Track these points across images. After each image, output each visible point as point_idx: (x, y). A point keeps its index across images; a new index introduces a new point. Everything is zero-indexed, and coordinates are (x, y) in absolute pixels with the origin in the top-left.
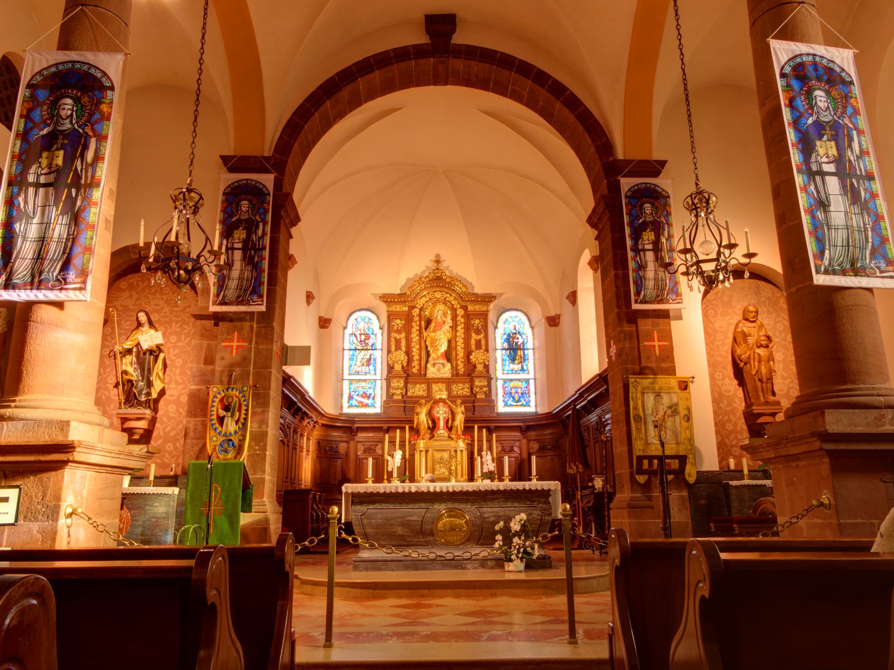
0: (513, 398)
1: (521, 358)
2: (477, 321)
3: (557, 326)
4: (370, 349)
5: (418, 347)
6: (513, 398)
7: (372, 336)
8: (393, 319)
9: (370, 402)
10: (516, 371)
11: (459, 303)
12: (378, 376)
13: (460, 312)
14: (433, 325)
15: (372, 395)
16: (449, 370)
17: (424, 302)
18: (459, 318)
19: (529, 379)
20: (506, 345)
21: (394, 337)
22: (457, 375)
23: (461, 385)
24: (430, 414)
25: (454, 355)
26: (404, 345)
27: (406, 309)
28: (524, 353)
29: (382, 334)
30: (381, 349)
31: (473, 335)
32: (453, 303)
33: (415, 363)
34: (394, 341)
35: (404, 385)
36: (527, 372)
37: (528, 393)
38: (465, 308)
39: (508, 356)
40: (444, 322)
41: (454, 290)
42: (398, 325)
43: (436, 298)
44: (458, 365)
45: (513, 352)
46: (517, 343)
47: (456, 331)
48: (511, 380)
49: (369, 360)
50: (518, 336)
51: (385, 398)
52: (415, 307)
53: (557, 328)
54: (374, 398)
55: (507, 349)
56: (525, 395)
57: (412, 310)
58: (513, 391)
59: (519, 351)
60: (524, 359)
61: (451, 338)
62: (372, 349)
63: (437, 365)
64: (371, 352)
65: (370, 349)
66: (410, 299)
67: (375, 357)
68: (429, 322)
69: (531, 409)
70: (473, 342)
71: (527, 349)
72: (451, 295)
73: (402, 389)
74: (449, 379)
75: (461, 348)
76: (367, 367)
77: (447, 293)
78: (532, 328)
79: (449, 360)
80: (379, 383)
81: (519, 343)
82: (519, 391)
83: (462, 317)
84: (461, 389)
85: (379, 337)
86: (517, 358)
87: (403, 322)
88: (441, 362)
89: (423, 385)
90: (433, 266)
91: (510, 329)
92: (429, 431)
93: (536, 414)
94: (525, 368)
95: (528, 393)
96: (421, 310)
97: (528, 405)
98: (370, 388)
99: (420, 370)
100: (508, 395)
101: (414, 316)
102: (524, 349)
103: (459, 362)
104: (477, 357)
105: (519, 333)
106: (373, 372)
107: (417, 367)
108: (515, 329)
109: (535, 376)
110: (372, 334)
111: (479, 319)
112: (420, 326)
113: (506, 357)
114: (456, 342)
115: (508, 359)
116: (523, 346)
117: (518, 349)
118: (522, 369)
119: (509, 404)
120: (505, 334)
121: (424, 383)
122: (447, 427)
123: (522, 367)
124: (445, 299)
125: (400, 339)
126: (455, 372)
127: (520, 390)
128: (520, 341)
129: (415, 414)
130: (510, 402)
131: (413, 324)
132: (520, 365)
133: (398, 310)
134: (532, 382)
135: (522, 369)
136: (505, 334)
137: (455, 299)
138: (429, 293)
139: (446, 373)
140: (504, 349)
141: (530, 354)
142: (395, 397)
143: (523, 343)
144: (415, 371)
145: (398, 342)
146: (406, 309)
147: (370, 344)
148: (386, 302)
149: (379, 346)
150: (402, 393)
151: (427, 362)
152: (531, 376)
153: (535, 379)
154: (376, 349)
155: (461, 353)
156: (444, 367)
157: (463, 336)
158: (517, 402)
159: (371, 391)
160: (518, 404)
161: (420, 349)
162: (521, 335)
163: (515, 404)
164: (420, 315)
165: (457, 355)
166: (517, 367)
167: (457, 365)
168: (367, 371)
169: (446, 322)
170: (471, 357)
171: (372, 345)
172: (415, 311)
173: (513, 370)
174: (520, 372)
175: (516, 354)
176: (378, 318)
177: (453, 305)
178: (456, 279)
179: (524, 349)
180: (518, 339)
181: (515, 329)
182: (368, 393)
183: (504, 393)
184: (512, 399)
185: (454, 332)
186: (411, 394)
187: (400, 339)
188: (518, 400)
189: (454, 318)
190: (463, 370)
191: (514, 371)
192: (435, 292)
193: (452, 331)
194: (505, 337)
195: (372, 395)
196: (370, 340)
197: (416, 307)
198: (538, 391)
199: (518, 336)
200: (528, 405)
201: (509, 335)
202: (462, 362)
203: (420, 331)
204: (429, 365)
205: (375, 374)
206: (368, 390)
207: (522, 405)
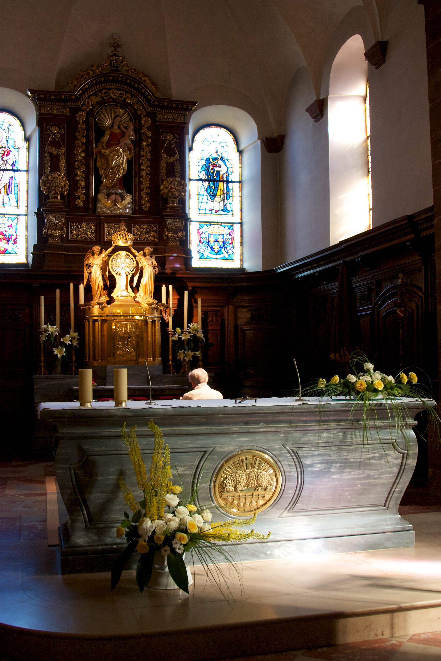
0: (212, 248)
1: (224, 193)
2: (170, 137)
3: (277, 152)
4: (9, 170)
5: (83, 168)
6: (212, 248)
7: (12, 150)
8: (47, 125)
9: (10, 246)
10: (217, 211)
11: (144, 108)
12: (23, 210)
13: (146, 122)
14: (106, 138)
15: (14, 238)
16: (129, 203)
17: (94, 103)
18: (144, 130)
19: (233, 223)
20: (204, 175)
21: (49, 153)
22: (141, 211)
23: (145, 227)
24: (105, 267)
25: (137, 183)
26: (63, 165)
27: (67, 112)
28: (227, 187)
29: (29, 149)
30: (27, 171)
31: (164, 156)
32: (136, 108)
33: (80, 192)
34: (48, 158)
35: (64, 224)
36: (231, 213)
37: (232, 242)
38: (152, 116)
39: (207, 191)
40: (123, 134)
41: (138, 88)
42: (54, 134)
43: (111, 97)
44: (142, 197)
45: (214, 184)
46: (218, 172)
47: (141, 149)
48: (210, 223)
49: (10, 184)
50: (220, 162)
51: (33, 241)
52: (80, 109)
53: (277, 154)
54: (15, 242)
55: (205, 180)
56: (227, 245)
57: (77, 113)
58: (212, 239)
59: (221, 184)
60: (227, 195)
61: (132, 158)
62: (14, 170)
63: (113, 197)
64: (11, 174)
65: (9, 170)
66: (73, 97)
67: (17, 181)
68: (100, 132)
69: (235, 264)
70: (163, 165)
71: (232, 182)
72: (133, 96)
73: (62, 230)
74: (129, 217)
75: (147, 174)
76: (6, 196)
77: (127, 92)
78: (240, 152)
79: (129, 191)
80: (23, 219)
81: (221, 173)
82: (220, 240)
83: (149, 128)
84: (146, 233)
85: (24, 153)
86: (219, 193)
87: (63, 131)
88: (120, 191)
89: (92, 225)
90: (109, 51)
91: (210, 153)
92: (105, 292)
93: (242, 271)
94: (228, 207)
95: (232, 242)
96: (90, 114)
97: (230, 258)
98: (10, 226)
99: (86, 202)
100: (205, 244)
101: (79, 123)
102: (228, 182)
103: (143, 194)
104: (171, 188)
105: (222, 158)
106: (14, 203)
107: (83, 198)
108: (217, 152)
109: (241, 219)
110: (14, 148)
111: (173, 134)
112: (87, 137)
113: (203, 192)
114: (140, 164)
115: (206, 193)
116: (227, 176)
117: (219, 181)
118: (225, 209)
119: (205, 255)
120: (202, 159)
121: (92, 222)
122: (132, 287)
123: (225, 206)
124: (125, 99)
125: (58, 156)
126: (137, 208)
127: (221, 237)
128: (223, 170)
129: (85, 268)
130: (208, 253)
131: (77, 134)
132: (222, 204)
133: (55, 112)
134: (237, 228)
135: (225, 209)
136: (202, 159)
137: (139, 102)
138: (101, 91)
139: (125, 208)
140: (201, 180)
141: (235, 188)
142: (51, 241)
143: (227, 172)
144: (80, 203)
145: (55, 160)
146: (67, 112)
147: (11, 162)
148: (39, 99)
149: (23, 165)
150: (61, 235)
151: (97, 191)
152: (237, 219)
153: (241, 224)
154: (18, 170)
155: (146, 182)
156: (123, 199)
157: (149, 156)
158: (216, 254)
159: (11, 231)
160: (218, 257)
161: (87, 172)
162: (224, 162)
163: (215, 257)
164: (86, 122)
165: (140, 183)
166: (218, 206)
167: (141, 198)
168: (6, 201)
169: (127, 135)
170: (162, 187)
171: (13, 164)
172: (81, 116)
173: (212, 210)
174: (222, 213)
175: (217, 188)
176: (23, 124)
177: (136, 110)
178: (143, 73)
179: (228, 182)
180: (220, 167)
181: (217, 152)
182: (7, 234)
183: (200, 241)
184: (210, 249)
185: (137, 149)
186: (75, 237)
187: (58, 156)
188: (218, 251)
189: (137, 130)
190: (148, 205)
191: (214, 212)
192: (109, 89)
193: (135, 149)
194: (203, 162)
195: (14, 238)
196: (11, 156)
197: (83, 111)
198: (245, 240)
199: (220, 162)
200: (230, 258)
201: (208, 160)
202: (147, 194)
203: (88, 144)
204: (101, 196)
205: (18, 206)
206: (8, 229)
207: (224, 259)
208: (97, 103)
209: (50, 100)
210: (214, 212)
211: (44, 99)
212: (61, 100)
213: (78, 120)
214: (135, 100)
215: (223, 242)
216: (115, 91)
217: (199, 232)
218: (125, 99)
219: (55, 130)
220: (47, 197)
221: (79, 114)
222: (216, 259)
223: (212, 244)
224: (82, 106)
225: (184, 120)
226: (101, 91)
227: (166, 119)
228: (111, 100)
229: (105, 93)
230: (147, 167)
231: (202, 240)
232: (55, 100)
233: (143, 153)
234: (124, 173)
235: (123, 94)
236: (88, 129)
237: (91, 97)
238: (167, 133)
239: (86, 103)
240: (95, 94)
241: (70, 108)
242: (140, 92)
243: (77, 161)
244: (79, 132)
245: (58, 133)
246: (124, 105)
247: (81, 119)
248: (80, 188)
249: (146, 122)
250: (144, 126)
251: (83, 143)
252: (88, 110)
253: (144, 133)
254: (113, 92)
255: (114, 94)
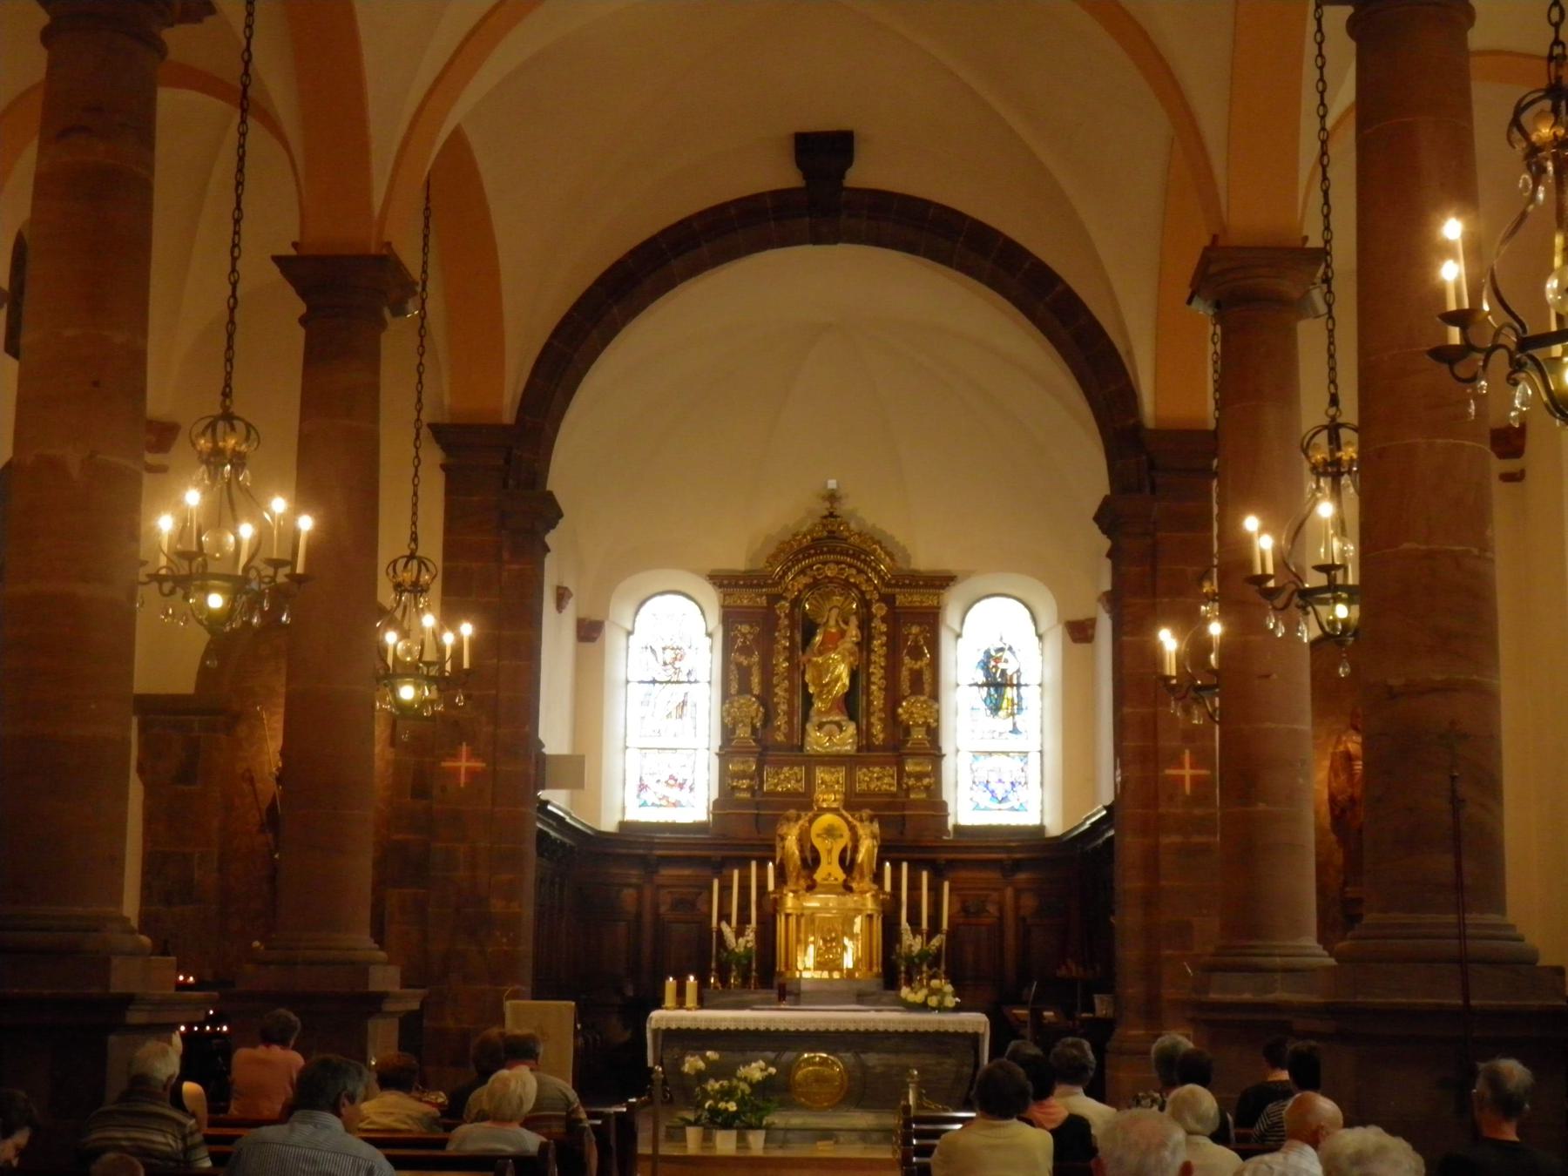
0: (992, 792)
2: (915, 630)
6: (992, 792)
10: (1001, 734)
13: (879, 609)
17: (801, 587)
26: (756, 680)
27: (763, 601)
31: (907, 659)
32: (864, 589)
43: (827, 577)
47: (870, 651)
52: (780, 597)
57: (776, 604)
66: (770, 581)
95: (1026, 783)
101: (779, 618)
112: (791, 639)
118: (1015, 731)
123: (1014, 724)
131: (777, 634)
145: (744, 673)
158: (1000, 802)
161: (791, 691)
164: (790, 616)
172: (782, 607)
183: (974, 783)
185: (865, 653)
187: (749, 667)
189: (865, 625)
197: (785, 599)
203: (792, 650)
208: (806, 586)
209: (737, 586)
210: (996, 735)
211: (729, 586)
212: (752, 586)
213: (778, 612)
214: (862, 578)
215: (1012, 784)
216: (832, 566)
217: (972, 769)
218: (847, 577)
219: (745, 629)
220: (733, 731)
221: (778, 605)
222: (1000, 810)
223: (991, 786)
224: (784, 592)
225: (938, 603)
226: (811, 567)
227: (911, 602)
228: (827, 580)
229: (818, 569)
230: (880, 679)
231: (976, 780)
232: (745, 586)
233: (873, 658)
234: (845, 691)
235: (844, 569)
236: (792, 627)
237: (798, 578)
238: (913, 624)
239: (790, 587)
240: (802, 572)
241: (767, 595)
242: (869, 565)
243: (777, 674)
244: (780, 631)
245: (749, 633)
246: (847, 585)
247: (782, 611)
248: (782, 714)
249: (879, 609)
250: (876, 616)
251: (785, 648)
252: (793, 597)
253: (875, 628)
254: (829, 568)
255: (830, 571)
